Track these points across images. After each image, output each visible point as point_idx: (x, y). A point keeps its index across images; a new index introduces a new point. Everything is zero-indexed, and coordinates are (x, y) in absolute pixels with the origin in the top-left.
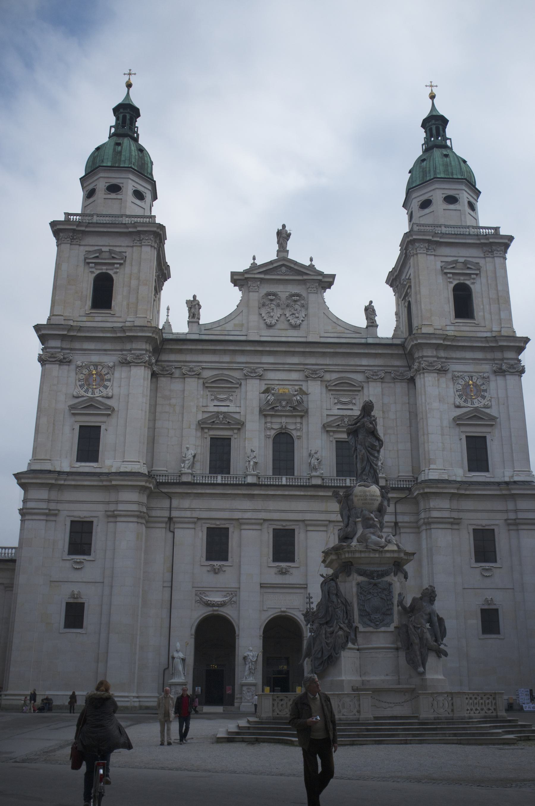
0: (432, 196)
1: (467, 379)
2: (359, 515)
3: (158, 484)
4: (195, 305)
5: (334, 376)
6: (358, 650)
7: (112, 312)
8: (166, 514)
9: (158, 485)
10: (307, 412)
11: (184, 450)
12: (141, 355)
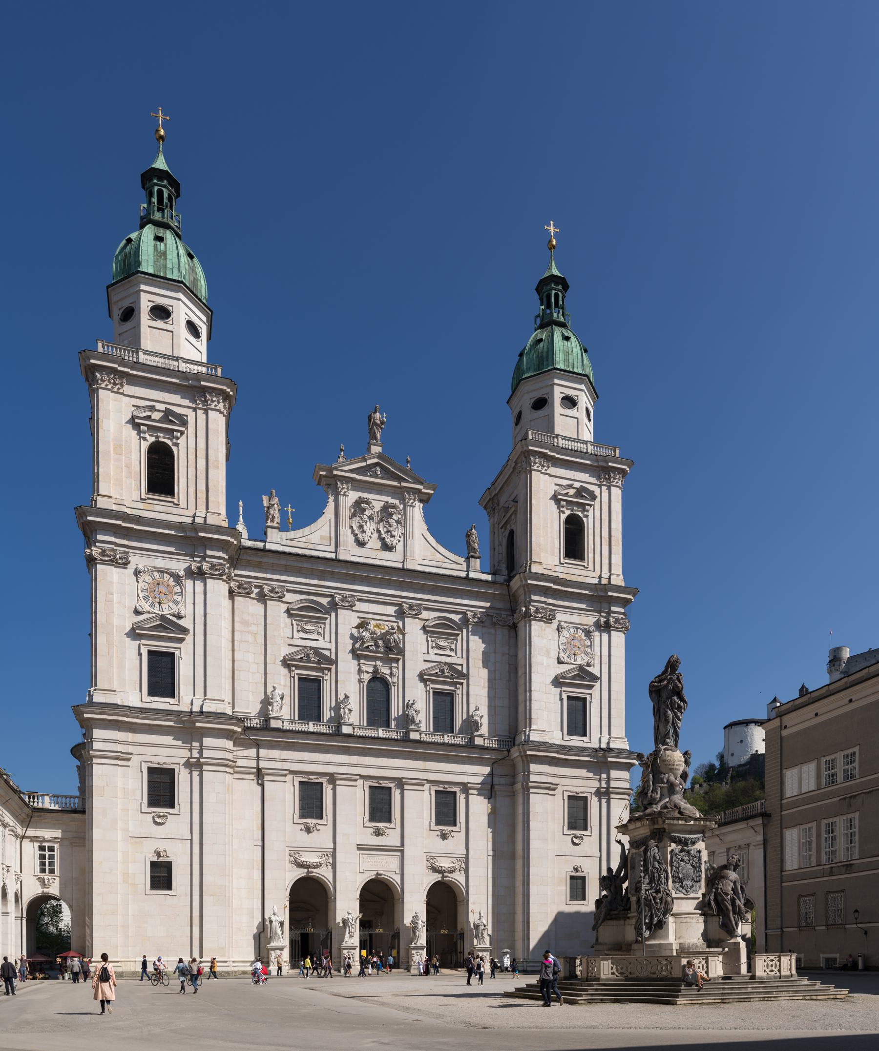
0: (548, 393)
1: (572, 630)
3: (245, 728)
4: (274, 504)
9: (245, 730)
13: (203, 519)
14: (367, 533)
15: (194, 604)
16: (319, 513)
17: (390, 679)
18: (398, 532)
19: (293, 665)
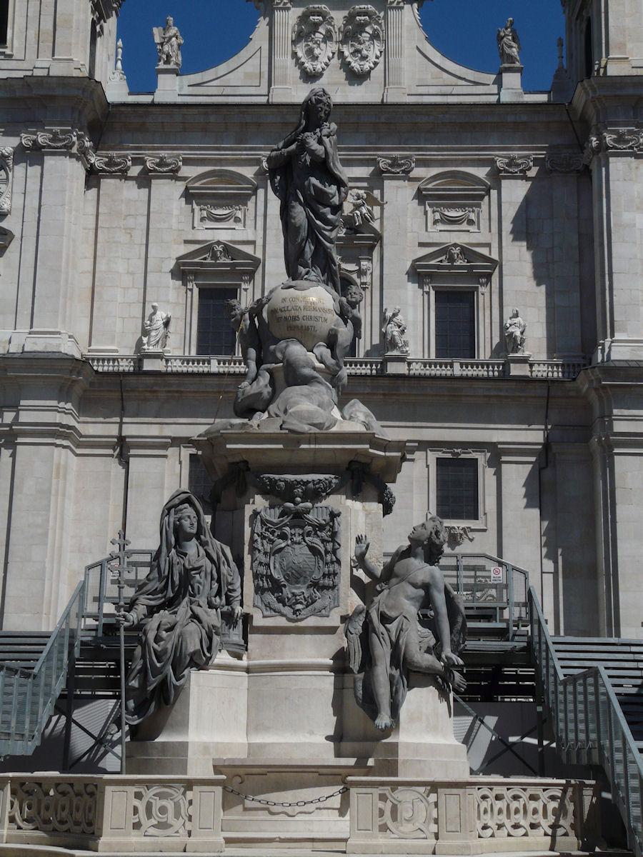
2: (279, 355)
4: (170, 38)
5: (435, 171)
6: (248, 670)
7: (8, 51)
8: (113, 430)
10: (378, 238)
11: (149, 311)
12: (64, 132)
13: (47, 70)
14: (320, 59)
15: (25, 194)
16: (243, 40)
17: (358, 281)
18: (373, 50)
19: (191, 272)
